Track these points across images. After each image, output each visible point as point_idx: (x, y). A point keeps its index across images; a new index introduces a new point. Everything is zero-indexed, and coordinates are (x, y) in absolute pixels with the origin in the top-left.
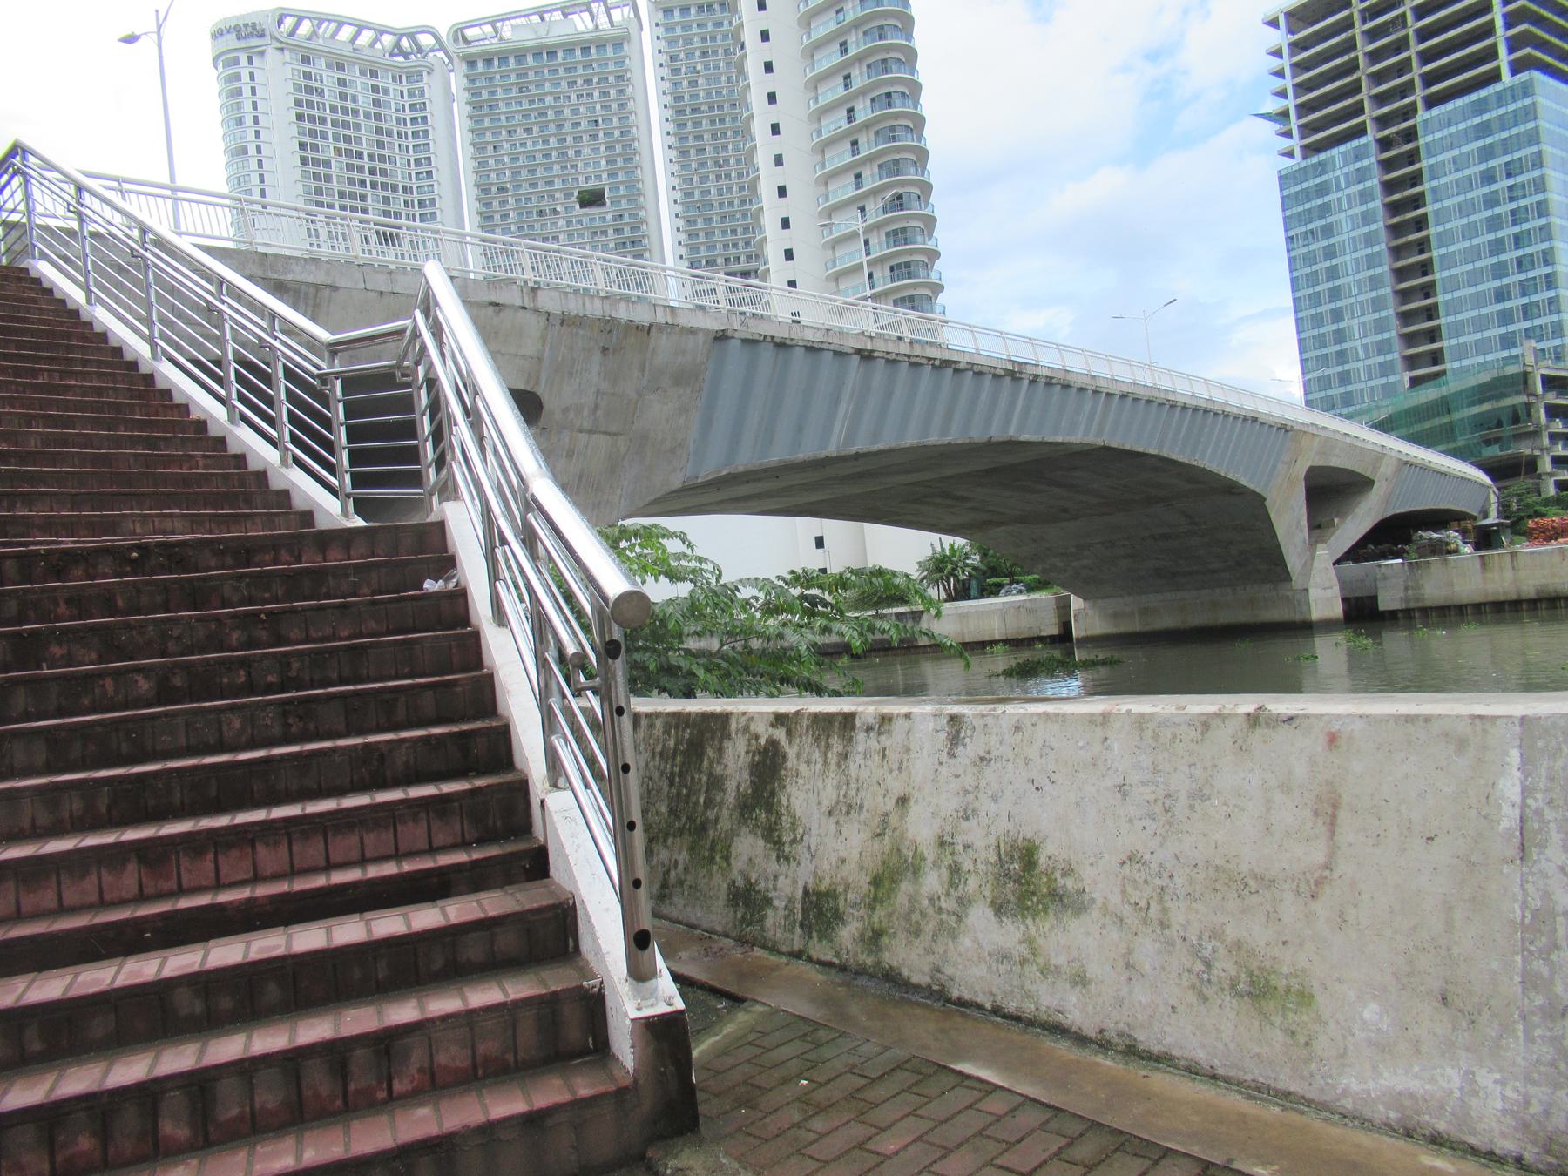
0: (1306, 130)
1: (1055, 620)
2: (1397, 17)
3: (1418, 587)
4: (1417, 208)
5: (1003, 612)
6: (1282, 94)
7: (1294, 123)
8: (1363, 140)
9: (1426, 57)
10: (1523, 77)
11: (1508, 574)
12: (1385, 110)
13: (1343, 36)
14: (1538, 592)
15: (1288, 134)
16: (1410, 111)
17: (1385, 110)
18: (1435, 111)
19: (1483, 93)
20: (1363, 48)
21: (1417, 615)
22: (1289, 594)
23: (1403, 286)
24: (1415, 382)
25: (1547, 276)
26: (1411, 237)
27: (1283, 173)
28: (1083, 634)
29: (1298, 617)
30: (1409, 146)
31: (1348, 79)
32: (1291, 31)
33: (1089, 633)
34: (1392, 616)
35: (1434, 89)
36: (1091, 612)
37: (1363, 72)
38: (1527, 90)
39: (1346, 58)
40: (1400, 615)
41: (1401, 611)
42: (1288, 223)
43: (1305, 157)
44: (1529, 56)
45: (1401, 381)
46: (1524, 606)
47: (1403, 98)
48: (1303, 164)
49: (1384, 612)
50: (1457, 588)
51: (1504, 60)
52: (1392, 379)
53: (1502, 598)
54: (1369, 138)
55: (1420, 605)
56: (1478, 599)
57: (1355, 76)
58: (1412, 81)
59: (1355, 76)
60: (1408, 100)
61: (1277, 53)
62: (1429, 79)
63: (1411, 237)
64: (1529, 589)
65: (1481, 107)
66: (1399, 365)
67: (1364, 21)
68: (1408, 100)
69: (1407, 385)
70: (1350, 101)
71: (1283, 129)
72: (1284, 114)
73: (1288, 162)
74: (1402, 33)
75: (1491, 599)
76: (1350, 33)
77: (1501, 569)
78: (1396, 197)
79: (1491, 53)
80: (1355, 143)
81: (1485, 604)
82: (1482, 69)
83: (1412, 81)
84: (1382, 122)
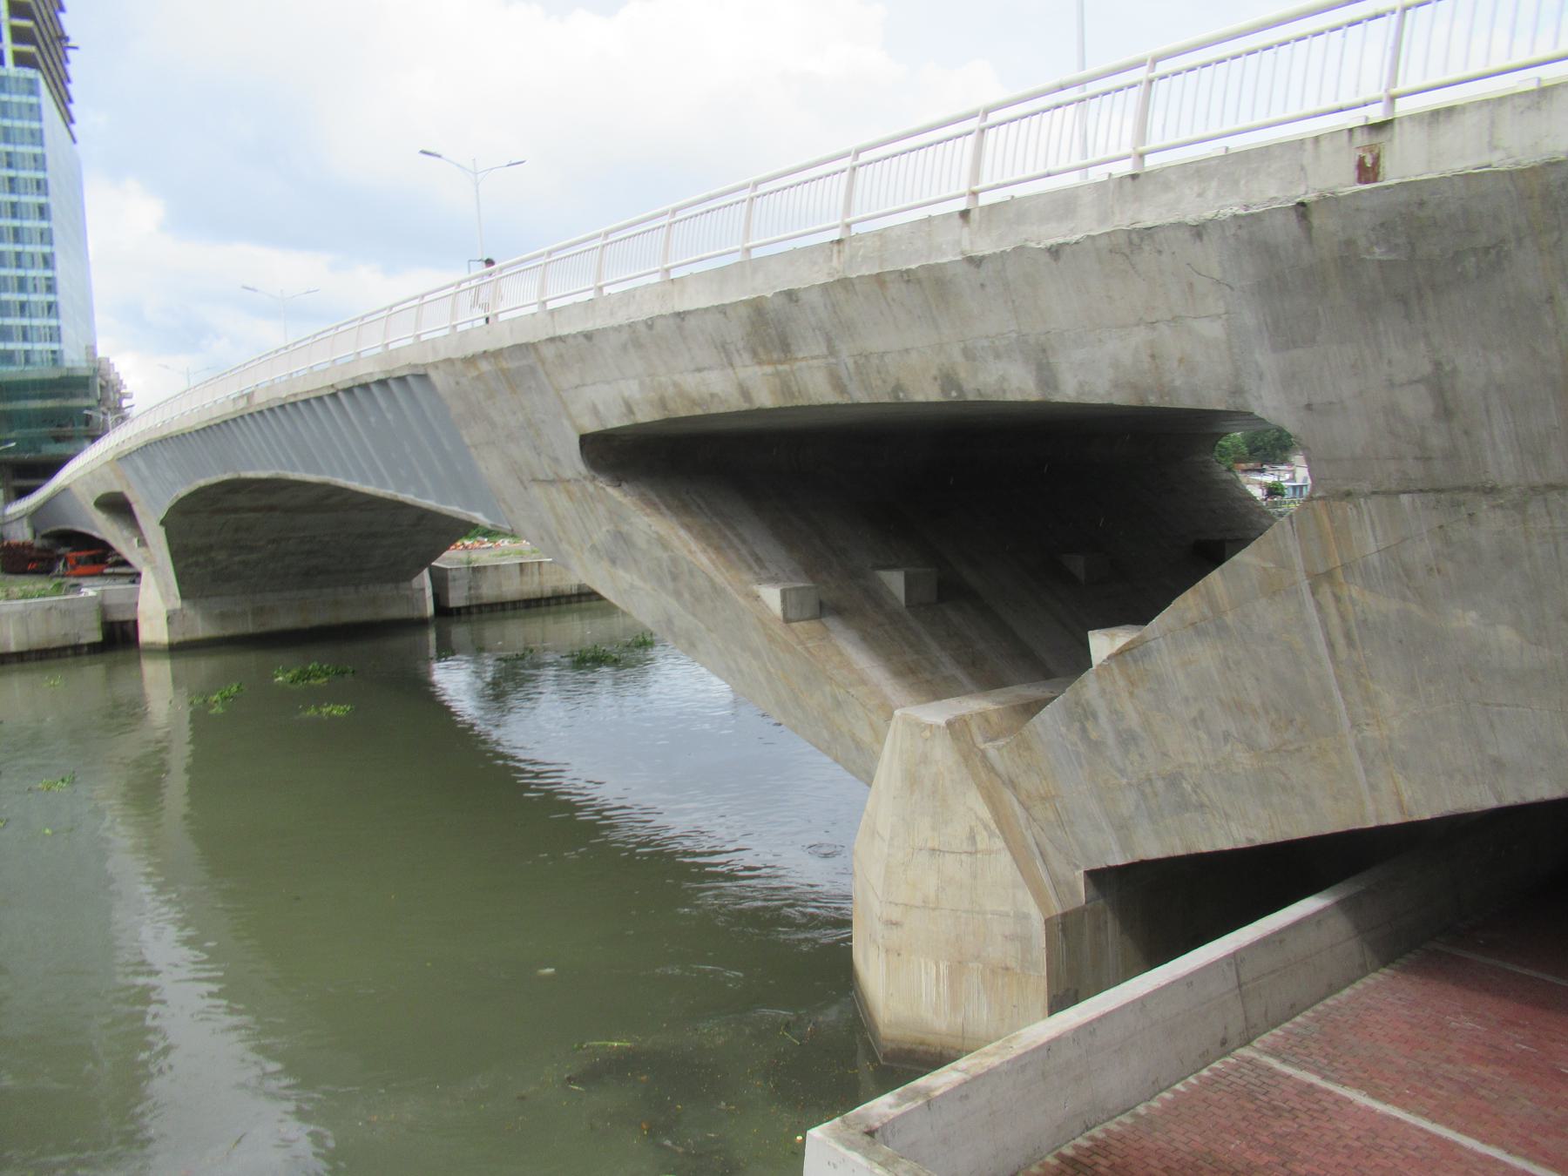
1: (97, 624)
3: (478, 587)
5: (24, 617)
10: (30, 73)
11: (536, 578)
14: (554, 591)
21: (475, 610)
22: (408, 593)
25: (48, 279)
28: (179, 638)
29: (416, 614)
33: (188, 637)
34: (459, 610)
36: (190, 613)
40: (463, 611)
41: (464, 607)
46: (543, 603)
49: (452, 609)
50: (504, 589)
53: (532, 596)
55: (479, 602)
56: (516, 597)
64: (548, 592)
75: (526, 597)
77: (532, 574)
81: (520, 601)
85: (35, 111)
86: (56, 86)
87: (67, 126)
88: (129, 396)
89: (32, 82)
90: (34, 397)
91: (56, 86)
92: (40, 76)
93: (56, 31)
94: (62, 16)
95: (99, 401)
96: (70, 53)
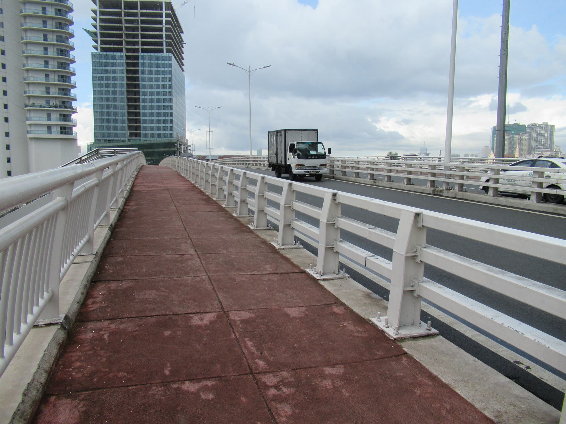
0: (103, 42)
2: (136, 20)
4: (135, 81)
6: (95, 27)
7: (99, 39)
8: (122, 54)
9: (143, 36)
10: (170, 55)
12: (129, 47)
13: (118, 17)
15: (96, 42)
16: (137, 51)
17: (129, 47)
18: (145, 54)
19: (159, 54)
20: (124, 25)
23: (130, 104)
24: (131, 135)
26: (134, 90)
27: (94, 53)
30: (136, 61)
31: (118, 32)
32: (100, 8)
35: (145, 47)
37: (124, 32)
38: (170, 59)
39: (118, 25)
42: (94, 71)
43: (101, 51)
44: (171, 49)
45: (127, 133)
47: (134, 45)
48: (101, 53)
51: (165, 48)
52: (124, 132)
54: (124, 54)
57: (121, 32)
58: (138, 42)
59: (121, 32)
60: (136, 47)
61: (95, 12)
62: (144, 44)
63: (134, 90)
65: (157, 58)
66: (127, 128)
67: (125, 16)
68: (136, 47)
69: (129, 135)
70: (118, 39)
71: (95, 39)
72: (96, 34)
73: (95, 51)
74: (137, 26)
76: (121, 18)
78: (130, 75)
79: (161, 44)
80: (119, 54)
82: (159, 47)
83: (138, 42)
84: (128, 50)
85: (170, 66)
86: (178, 56)
87: (181, 67)
88: (190, 146)
89: (170, 57)
90: (162, 148)
91: (178, 56)
92: (172, 55)
93: (179, 40)
94: (182, 34)
95: (178, 149)
96: (184, 45)
